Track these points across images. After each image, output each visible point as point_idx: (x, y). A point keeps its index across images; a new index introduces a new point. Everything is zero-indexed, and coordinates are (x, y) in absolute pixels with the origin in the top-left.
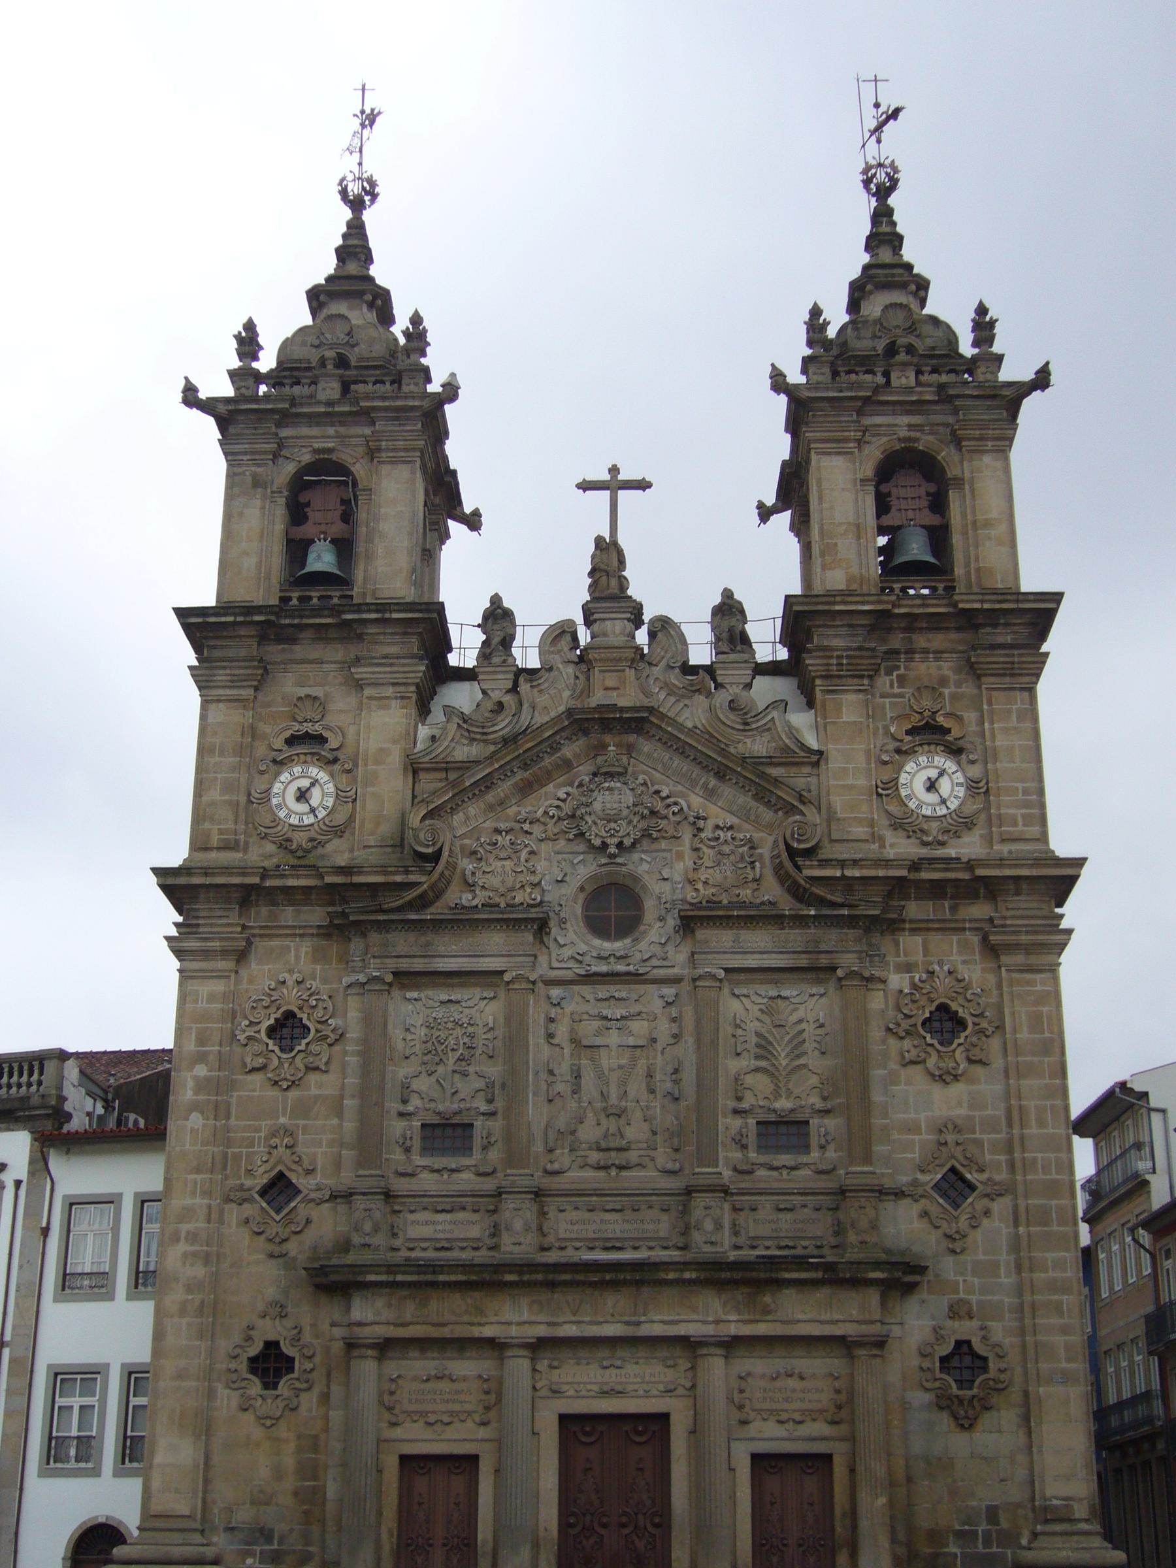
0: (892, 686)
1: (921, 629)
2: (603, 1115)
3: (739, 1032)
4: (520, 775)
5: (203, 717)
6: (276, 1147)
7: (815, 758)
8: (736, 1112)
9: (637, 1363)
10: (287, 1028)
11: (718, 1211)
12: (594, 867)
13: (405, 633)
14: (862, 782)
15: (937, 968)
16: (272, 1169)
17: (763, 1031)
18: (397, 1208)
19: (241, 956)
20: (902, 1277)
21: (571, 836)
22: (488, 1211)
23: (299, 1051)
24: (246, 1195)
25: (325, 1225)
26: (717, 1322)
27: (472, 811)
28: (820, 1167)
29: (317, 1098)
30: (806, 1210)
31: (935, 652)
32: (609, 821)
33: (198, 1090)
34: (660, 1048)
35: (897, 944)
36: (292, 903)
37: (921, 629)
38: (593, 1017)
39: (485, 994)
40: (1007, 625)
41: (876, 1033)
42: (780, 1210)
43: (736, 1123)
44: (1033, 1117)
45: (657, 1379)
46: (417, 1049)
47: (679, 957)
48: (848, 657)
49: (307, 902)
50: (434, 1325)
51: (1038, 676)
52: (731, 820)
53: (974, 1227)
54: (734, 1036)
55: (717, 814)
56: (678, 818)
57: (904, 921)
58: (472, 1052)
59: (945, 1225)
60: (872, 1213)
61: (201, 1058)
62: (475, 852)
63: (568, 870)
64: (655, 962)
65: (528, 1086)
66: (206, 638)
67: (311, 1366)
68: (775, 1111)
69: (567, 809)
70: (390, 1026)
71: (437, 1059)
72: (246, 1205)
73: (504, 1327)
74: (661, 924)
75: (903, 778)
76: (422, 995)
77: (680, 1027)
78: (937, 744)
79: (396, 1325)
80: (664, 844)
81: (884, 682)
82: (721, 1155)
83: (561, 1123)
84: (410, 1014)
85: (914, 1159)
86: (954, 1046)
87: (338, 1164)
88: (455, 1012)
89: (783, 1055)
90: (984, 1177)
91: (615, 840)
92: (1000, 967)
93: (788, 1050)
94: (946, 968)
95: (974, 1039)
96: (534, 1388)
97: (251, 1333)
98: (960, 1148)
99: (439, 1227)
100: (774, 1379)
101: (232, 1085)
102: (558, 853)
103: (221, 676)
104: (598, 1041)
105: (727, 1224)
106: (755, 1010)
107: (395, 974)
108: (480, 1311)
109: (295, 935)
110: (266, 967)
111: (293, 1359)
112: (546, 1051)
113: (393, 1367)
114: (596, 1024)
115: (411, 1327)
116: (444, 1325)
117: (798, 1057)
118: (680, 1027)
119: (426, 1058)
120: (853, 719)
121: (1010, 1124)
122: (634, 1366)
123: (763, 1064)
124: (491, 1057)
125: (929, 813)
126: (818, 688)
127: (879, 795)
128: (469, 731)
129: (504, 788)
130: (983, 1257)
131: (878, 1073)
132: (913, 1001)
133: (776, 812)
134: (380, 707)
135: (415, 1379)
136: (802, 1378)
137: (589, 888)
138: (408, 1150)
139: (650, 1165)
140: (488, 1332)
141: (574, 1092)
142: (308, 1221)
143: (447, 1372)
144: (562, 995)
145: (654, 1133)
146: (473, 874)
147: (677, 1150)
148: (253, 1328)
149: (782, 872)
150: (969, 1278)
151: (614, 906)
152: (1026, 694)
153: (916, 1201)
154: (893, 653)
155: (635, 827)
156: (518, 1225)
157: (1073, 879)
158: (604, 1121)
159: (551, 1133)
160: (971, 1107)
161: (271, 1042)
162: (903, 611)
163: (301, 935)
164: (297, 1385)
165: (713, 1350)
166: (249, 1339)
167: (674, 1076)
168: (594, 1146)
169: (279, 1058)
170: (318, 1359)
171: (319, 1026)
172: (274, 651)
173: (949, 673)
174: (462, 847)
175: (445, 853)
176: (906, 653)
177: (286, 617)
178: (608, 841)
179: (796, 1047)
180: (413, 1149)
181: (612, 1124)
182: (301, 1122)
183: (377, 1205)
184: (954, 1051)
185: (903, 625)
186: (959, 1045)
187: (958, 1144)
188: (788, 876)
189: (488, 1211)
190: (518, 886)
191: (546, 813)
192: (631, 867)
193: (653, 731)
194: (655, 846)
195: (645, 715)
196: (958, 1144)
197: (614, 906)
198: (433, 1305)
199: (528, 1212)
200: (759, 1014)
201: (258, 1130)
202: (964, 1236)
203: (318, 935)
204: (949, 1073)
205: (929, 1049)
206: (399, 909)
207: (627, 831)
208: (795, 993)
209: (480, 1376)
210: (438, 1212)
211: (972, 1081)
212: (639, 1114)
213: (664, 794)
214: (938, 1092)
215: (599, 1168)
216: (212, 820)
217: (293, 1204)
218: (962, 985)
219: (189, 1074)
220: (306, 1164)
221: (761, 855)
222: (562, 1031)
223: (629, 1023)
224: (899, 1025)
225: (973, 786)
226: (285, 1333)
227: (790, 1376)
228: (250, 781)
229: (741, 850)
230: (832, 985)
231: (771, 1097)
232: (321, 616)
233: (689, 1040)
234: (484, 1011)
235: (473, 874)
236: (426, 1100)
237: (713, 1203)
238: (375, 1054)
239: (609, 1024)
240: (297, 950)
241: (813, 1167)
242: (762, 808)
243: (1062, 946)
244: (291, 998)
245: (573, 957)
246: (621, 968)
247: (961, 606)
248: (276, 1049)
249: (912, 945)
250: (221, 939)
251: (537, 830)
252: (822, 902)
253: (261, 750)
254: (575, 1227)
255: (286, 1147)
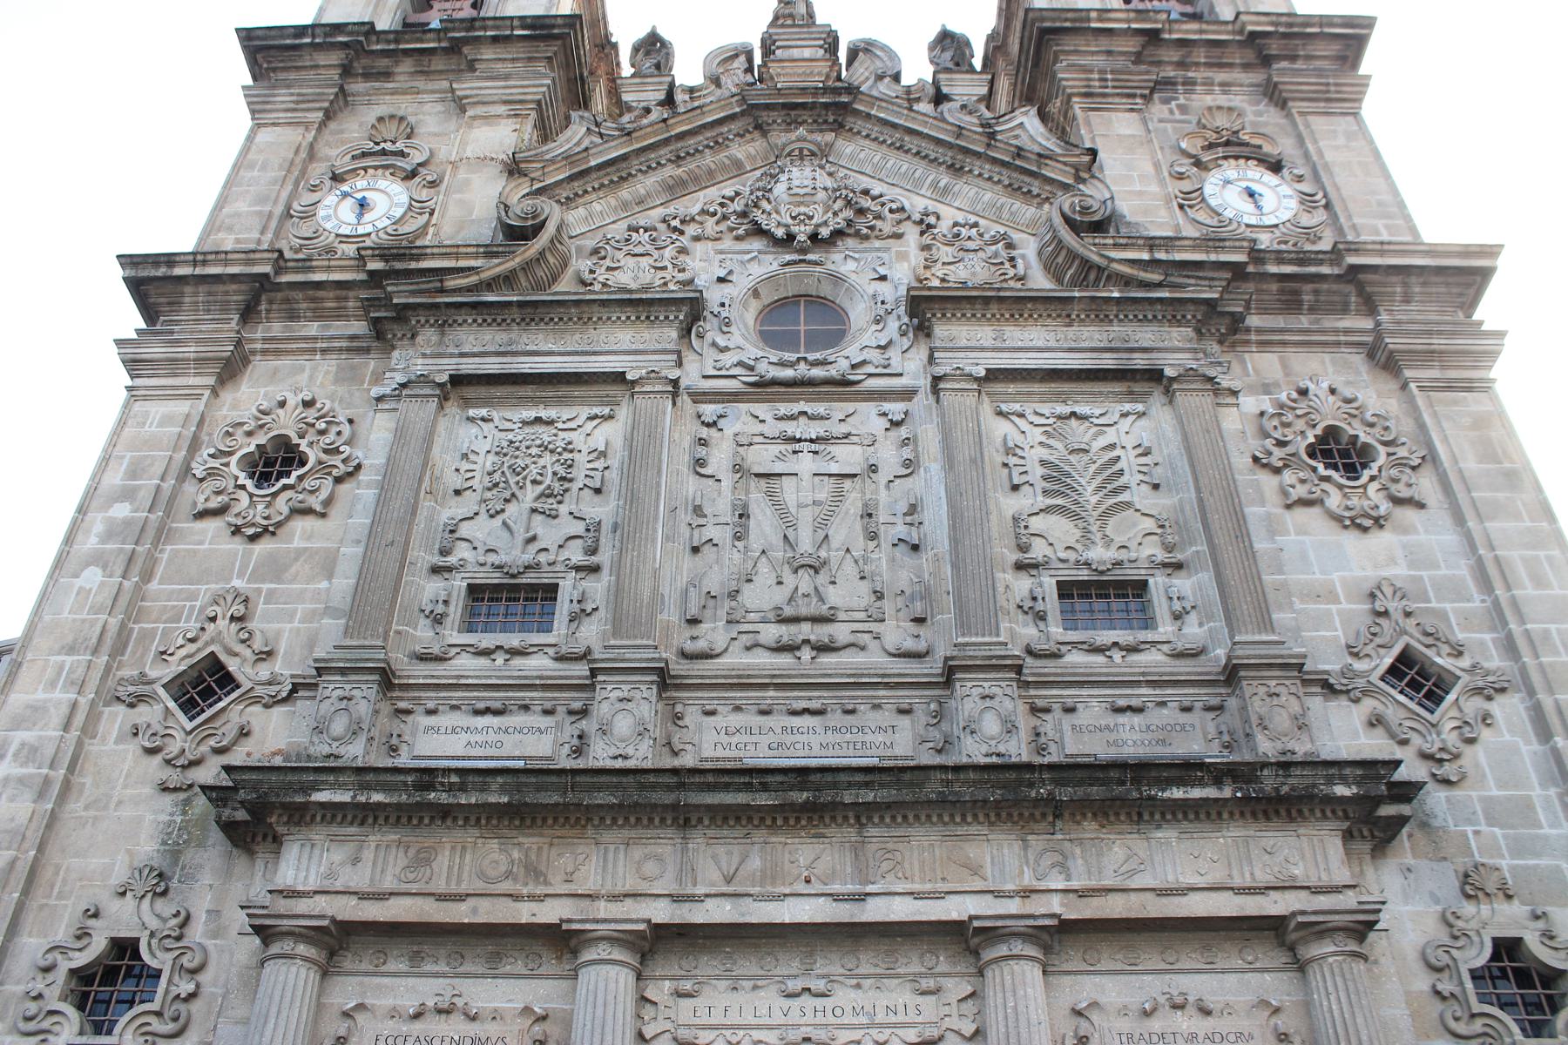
0: (1171, 112)
1: (1197, 64)
2: (787, 570)
3: (1012, 460)
4: (670, 171)
5: (250, 139)
6: (213, 619)
7: (1087, 159)
8: (1020, 567)
9: (858, 986)
10: (273, 463)
11: (1008, 704)
12: (775, 266)
13: (530, 59)
14: (1154, 188)
15: (1312, 387)
16: (199, 650)
17: (1052, 459)
18: (402, 705)
19: (230, 369)
20: (1375, 808)
21: (741, 232)
22: (571, 713)
23: (285, 487)
24: (140, 689)
25: (273, 735)
26: (1026, 893)
27: (597, 207)
28: (1180, 646)
29: (299, 553)
30: (1165, 711)
31: (1222, 84)
32: (799, 204)
33: (108, 536)
34: (884, 481)
35: (1243, 362)
36: (319, 314)
37: (1197, 64)
38: (772, 439)
39: (596, 410)
40: (1309, 58)
41: (1241, 462)
42: (1119, 710)
43: (1022, 585)
44: (1522, 572)
45: (900, 1018)
46: (475, 483)
47: (911, 366)
48: (1112, 72)
49: (340, 314)
50: (442, 898)
51: (1360, 101)
52: (973, 219)
53: (1471, 741)
54: (1005, 465)
55: (949, 215)
56: (897, 216)
57: (1248, 330)
58: (567, 485)
59: (1416, 740)
60: (1295, 706)
61: (127, 494)
62: (595, 251)
63: (737, 269)
64: (870, 369)
65: (656, 519)
66: (274, 70)
67: (191, 987)
68: (1087, 564)
69: (738, 206)
70: (436, 450)
71: (507, 494)
72: (142, 708)
73: (586, 903)
74: (879, 327)
75: (1208, 190)
76: (495, 414)
77: (915, 450)
78: (1248, 158)
79: (363, 896)
80: (877, 244)
81: (1158, 110)
82: (1004, 625)
83: (715, 582)
84: (472, 439)
85: (1336, 637)
86: (1365, 478)
87: (311, 644)
88: (545, 433)
89: (1090, 489)
90: (1465, 662)
91: (809, 229)
92: (1404, 387)
93: (1095, 483)
94: (1325, 385)
95: (1394, 472)
96: (641, 1035)
97: (92, 922)
98: (1412, 622)
99: (479, 738)
100: (1147, 1014)
101: (163, 534)
102: (721, 252)
103: (283, 97)
104: (779, 468)
105: (1024, 734)
106: (1036, 435)
107: (458, 380)
108: (535, 872)
109: (314, 351)
110: (262, 391)
111: (157, 975)
112: (692, 485)
113: (345, 992)
114: (775, 449)
115: (393, 901)
116: (460, 898)
117: (1116, 492)
118: (915, 450)
119: (488, 495)
120: (1128, 132)
121: (1485, 584)
122: (853, 994)
123: (1059, 501)
124: (598, 491)
125: (1253, 221)
126: (1076, 107)
127: (1181, 207)
128: (601, 135)
129: (646, 184)
130: (1495, 792)
131: (1253, 511)
132: (1288, 425)
133: (1040, 205)
134: (490, 125)
135: (394, 1013)
136: (1207, 1013)
137: (768, 296)
138: (438, 620)
139: (873, 645)
140: (548, 913)
141: (738, 537)
142: (244, 733)
143: (459, 1002)
144: (721, 412)
145: (879, 596)
146: (592, 272)
147: (920, 621)
148: (96, 915)
149: (1060, 260)
150: (1483, 828)
151: (804, 314)
152: (1350, 119)
153: (1356, 701)
154: (1169, 83)
155: (835, 214)
156: (623, 725)
157: (1485, 274)
158: (790, 580)
159: (693, 592)
160: (1412, 565)
161: (242, 475)
162: (1175, 36)
163: (324, 351)
164: (157, 1025)
165: (1018, 947)
166: (83, 934)
167: (908, 519)
168: (771, 616)
169: (251, 495)
170: (205, 978)
171: (324, 457)
172: (357, 86)
173: (1245, 106)
174: (579, 249)
175: (550, 229)
176: (1184, 84)
177: (378, 42)
178: (795, 229)
179: (1109, 479)
180: (448, 621)
181: (805, 581)
182: (265, 586)
183: (365, 694)
184: (1365, 487)
185: (1175, 59)
186: (1373, 478)
187: (1408, 614)
188: (1072, 255)
189: (571, 713)
190: (658, 282)
191: (703, 212)
192: (832, 267)
193: (859, 125)
194: (866, 245)
195: (845, 99)
196: (1408, 614)
197: (804, 314)
198: (443, 861)
199: (645, 703)
200: (1043, 439)
201: (193, 597)
202: (1456, 757)
203: (349, 350)
204: (1366, 516)
205: (1325, 486)
206: (469, 289)
207: (826, 219)
208: (1098, 412)
209: (527, 1010)
210: (477, 712)
211: (1405, 530)
212: (850, 569)
213: (875, 192)
214: (1351, 541)
215: (781, 648)
216: (230, 229)
217: (221, 705)
218: (1355, 405)
219: (100, 516)
220: (258, 644)
221: (1023, 257)
222: (720, 458)
223: (830, 448)
224: (1270, 454)
225: (1307, 200)
226: (154, 923)
227: (1181, 1007)
228: (294, 195)
229: (993, 248)
230: (1157, 402)
231: (1078, 546)
232: (422, 41)
233: (933, 468)
234: (594, 433)
235: (592, 272)
236: (481, 550)
237: (995, 690)
238: (408, 480)
239: (797, 447)
240: (314, 369)
241: (1165, 648)
242: (1017, 205)
243: (1493, 355)
244: (286, 424)
245: (740, 364)
246: (817, 372)
247: (1250, 28)
248: (249, 484)
249: (1266, 363)
250: (198, 341)
251: (691, 230)
252: (1127, 282)
253: (318, 171)
254: (735, 740)
255: (232, 618)
